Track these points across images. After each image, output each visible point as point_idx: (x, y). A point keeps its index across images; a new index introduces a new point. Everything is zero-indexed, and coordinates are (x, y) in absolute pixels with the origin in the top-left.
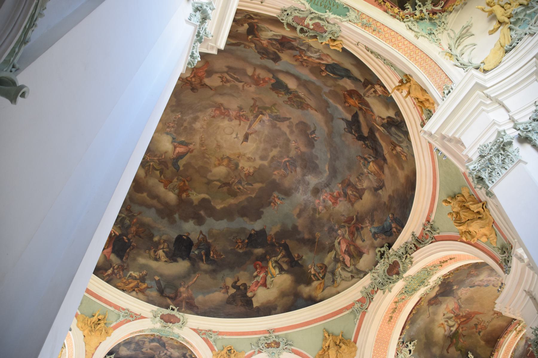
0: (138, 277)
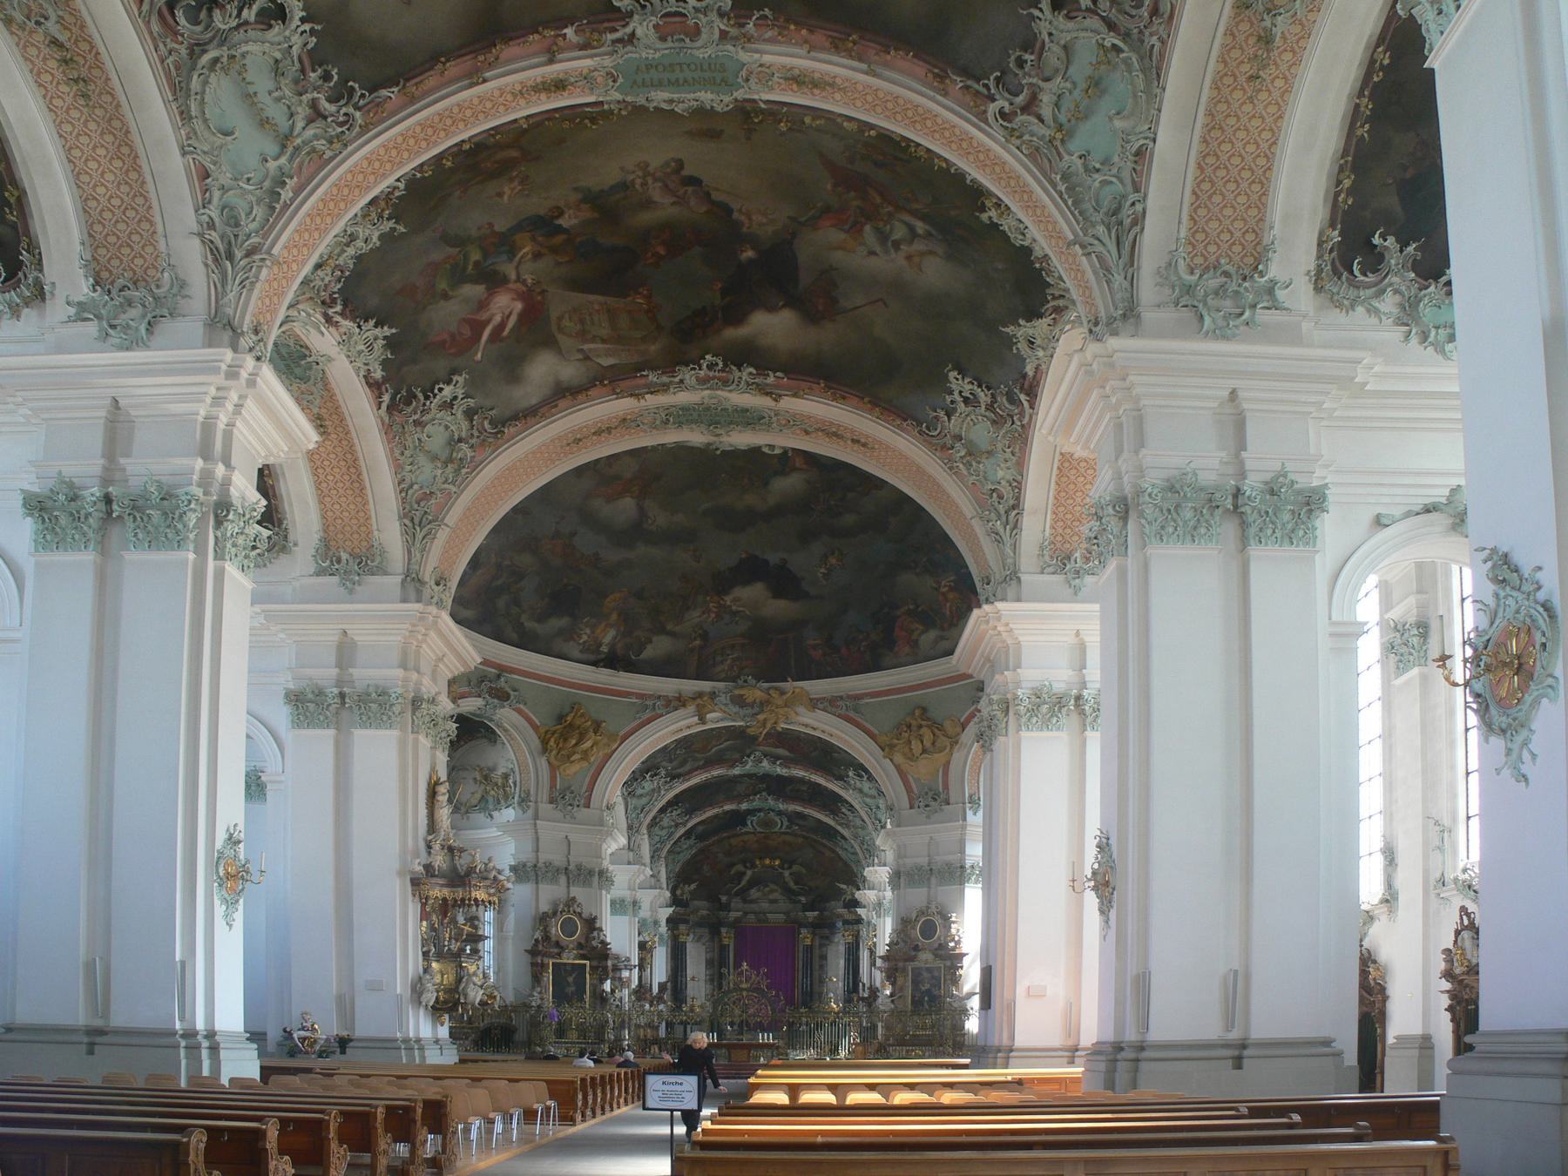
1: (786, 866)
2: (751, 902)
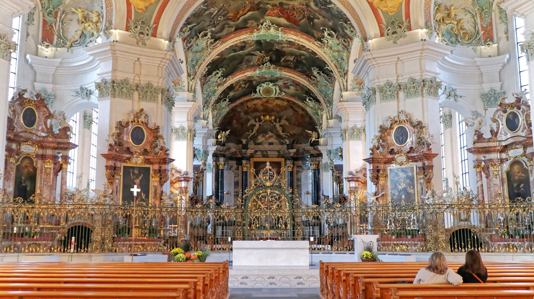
1: (278, 120)
2: (260, 144)
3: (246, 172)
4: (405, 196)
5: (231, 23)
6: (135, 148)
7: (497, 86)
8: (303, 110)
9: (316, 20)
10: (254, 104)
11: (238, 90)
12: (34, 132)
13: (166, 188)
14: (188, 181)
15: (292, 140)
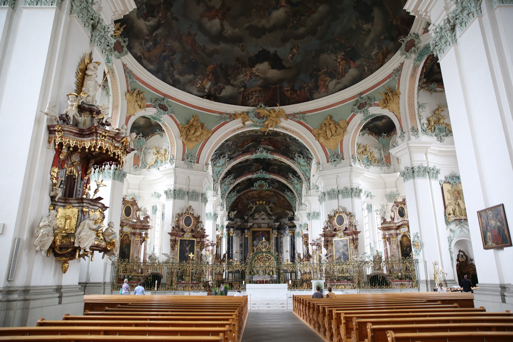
0: (377, 51)
1: (267, 204)
2: (256, 219)
3: (247, 238)
4: (343, 256)
5: (240, 149)
6: (186, 228)
7: (394, 190)
8: (284, 197)
9: (290, 148)
10: (252, 194)
11: (242, 185)
12: (131, 220)
13: (204, 252)
14: (213, 246)
15: (277, 217)
